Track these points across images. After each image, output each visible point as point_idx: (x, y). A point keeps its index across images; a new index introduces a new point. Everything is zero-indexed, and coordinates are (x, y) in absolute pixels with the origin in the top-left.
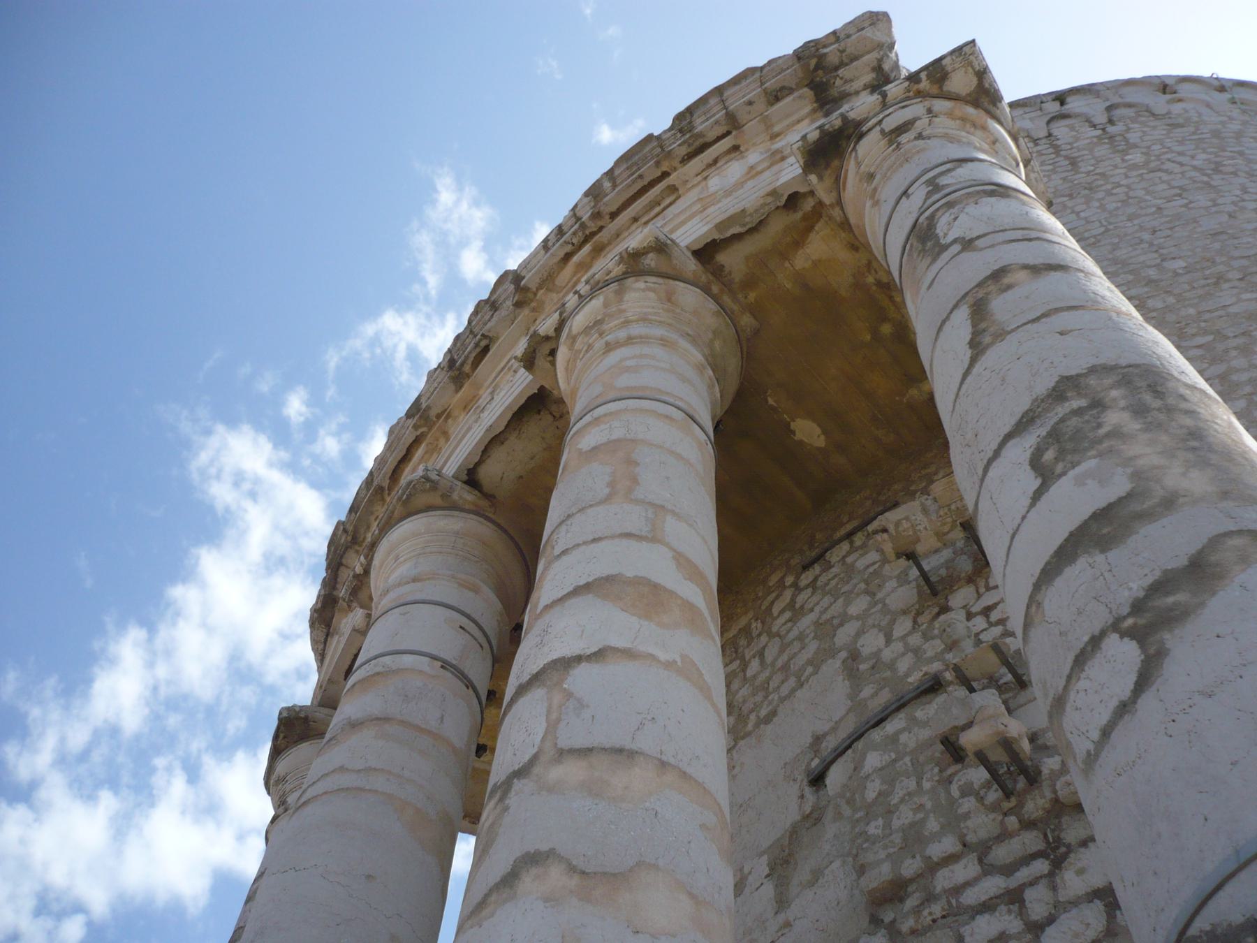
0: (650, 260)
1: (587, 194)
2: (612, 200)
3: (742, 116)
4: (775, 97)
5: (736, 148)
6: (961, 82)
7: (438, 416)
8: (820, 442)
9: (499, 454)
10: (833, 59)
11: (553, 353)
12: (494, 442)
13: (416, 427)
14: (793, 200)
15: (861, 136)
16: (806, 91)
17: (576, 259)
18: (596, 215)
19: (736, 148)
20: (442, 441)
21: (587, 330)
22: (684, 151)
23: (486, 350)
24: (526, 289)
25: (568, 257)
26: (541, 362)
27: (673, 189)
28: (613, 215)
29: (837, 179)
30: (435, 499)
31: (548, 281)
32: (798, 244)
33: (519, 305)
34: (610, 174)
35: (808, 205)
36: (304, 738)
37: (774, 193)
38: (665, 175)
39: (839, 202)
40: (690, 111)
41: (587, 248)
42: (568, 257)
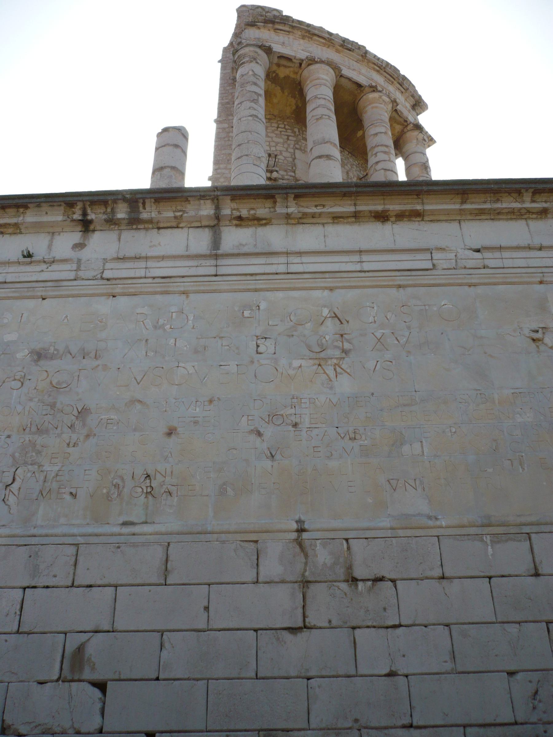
0: (395, 104)
1: (386, 62)
2: (388, 70)
3: (408, 91)
4: (413, 96)
5: (402, 92)
6: (431, 143)
7: (332, 43)
8: (358, 136)
9: (347, 81)
10: (421, 104)
11: (374, 91)
12: (350, 79)
13: (328, 38)
14: (406, 121)
15: (421, 132)
16: (415, 103)
18: (384, 68)
19: (402, 92)
20: (327, 46)
21: (384, 101)
22: (400, 82)
23: (350, 50)
24: (366, 56)
25: (375, 64)
26: (372, 89)
27: (393, 83)
28: (385, 71)
29: (413, 130)
30: (337, 72)
31: (369, 61)
32: (398, 124)
33: (362, 56)
34: (391, 65)
35: (406, 124)
36: (267, 53)
37: (407, 118)
38: (395, 79)
39: (408, 131)
40: (406, 78)
41: (378, 68)
42: (375, 64)
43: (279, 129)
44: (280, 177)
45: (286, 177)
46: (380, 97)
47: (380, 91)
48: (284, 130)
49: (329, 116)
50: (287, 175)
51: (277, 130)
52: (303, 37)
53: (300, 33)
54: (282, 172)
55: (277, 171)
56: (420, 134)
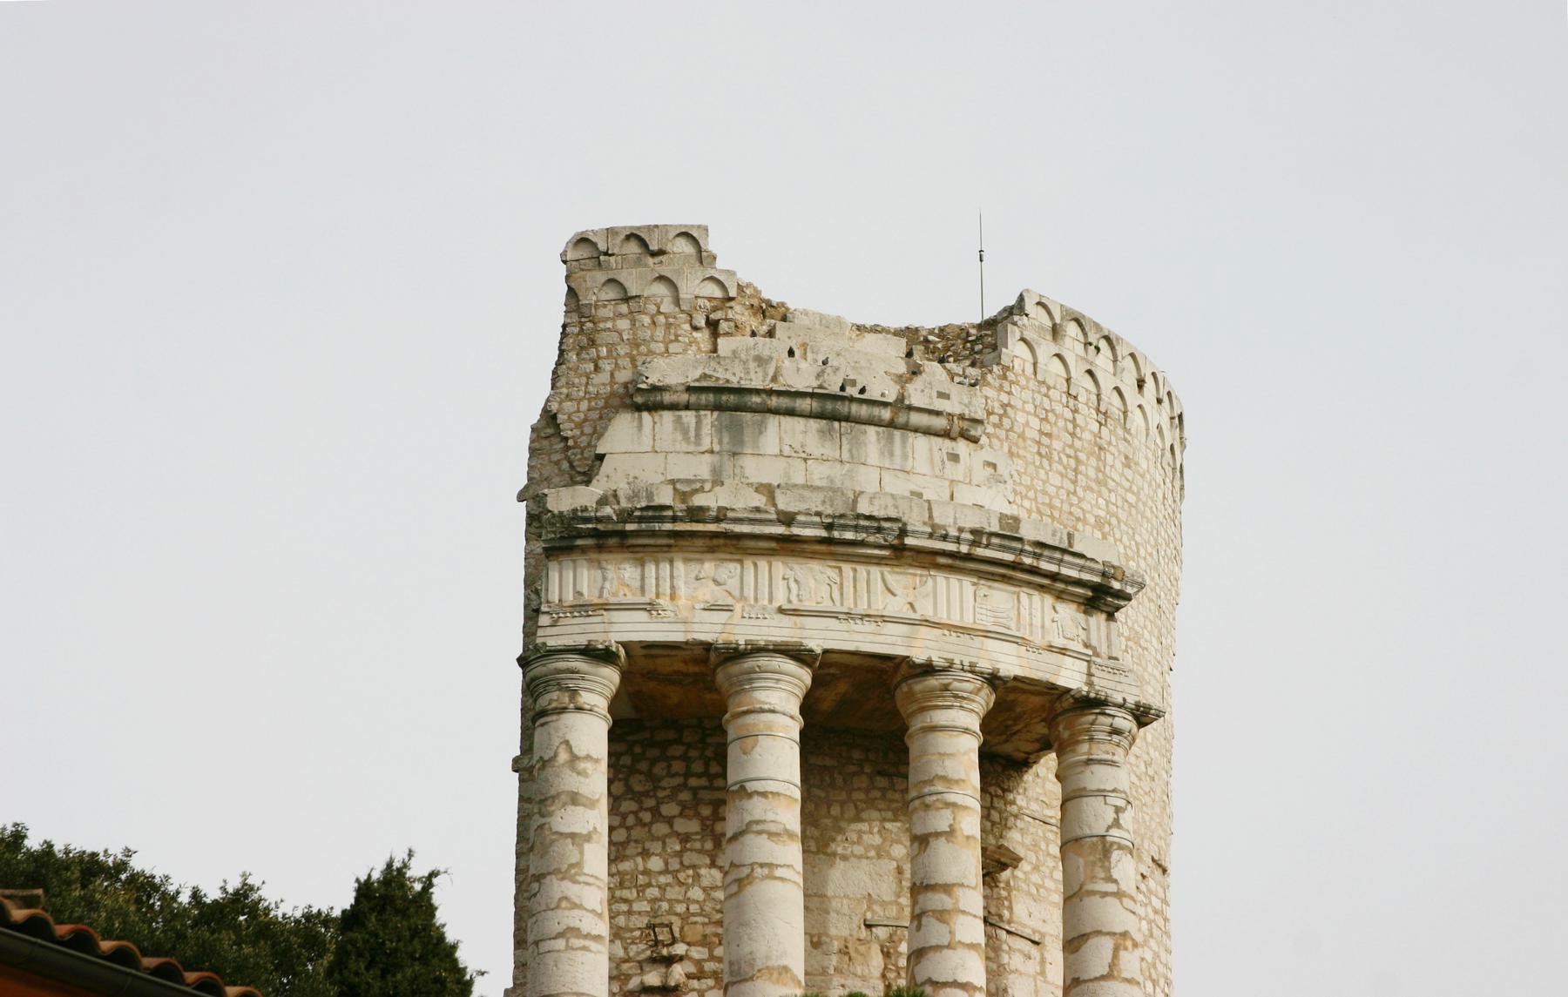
15: (1104, 714)
17: (942, 560)
41: (950, 561)
43: (693, 782)
44: (692, 969)
45: (710, 966)
46: (946, 688)
47: (944, 670)
48: (703, 782)
49: (770, 865)
50: (712, 958)
51: (684, 786)
52: (712, 550)
53: (700, 542)
54: (698, 953)
55: (681, 959)
56: (1101, 719)
